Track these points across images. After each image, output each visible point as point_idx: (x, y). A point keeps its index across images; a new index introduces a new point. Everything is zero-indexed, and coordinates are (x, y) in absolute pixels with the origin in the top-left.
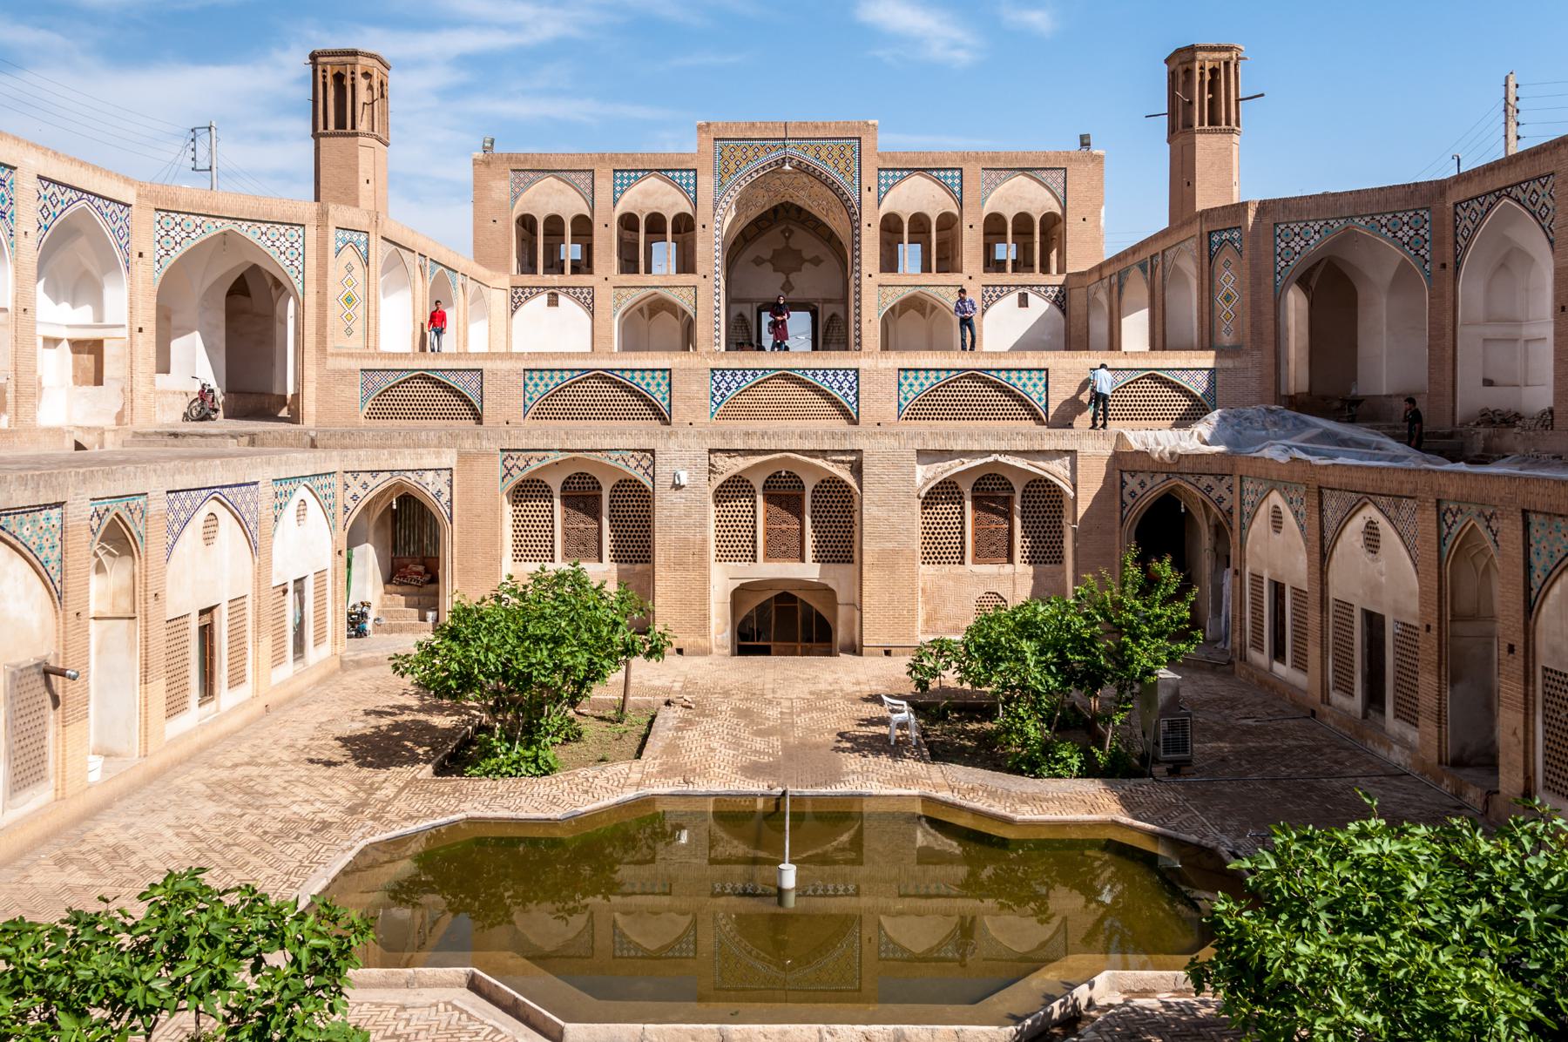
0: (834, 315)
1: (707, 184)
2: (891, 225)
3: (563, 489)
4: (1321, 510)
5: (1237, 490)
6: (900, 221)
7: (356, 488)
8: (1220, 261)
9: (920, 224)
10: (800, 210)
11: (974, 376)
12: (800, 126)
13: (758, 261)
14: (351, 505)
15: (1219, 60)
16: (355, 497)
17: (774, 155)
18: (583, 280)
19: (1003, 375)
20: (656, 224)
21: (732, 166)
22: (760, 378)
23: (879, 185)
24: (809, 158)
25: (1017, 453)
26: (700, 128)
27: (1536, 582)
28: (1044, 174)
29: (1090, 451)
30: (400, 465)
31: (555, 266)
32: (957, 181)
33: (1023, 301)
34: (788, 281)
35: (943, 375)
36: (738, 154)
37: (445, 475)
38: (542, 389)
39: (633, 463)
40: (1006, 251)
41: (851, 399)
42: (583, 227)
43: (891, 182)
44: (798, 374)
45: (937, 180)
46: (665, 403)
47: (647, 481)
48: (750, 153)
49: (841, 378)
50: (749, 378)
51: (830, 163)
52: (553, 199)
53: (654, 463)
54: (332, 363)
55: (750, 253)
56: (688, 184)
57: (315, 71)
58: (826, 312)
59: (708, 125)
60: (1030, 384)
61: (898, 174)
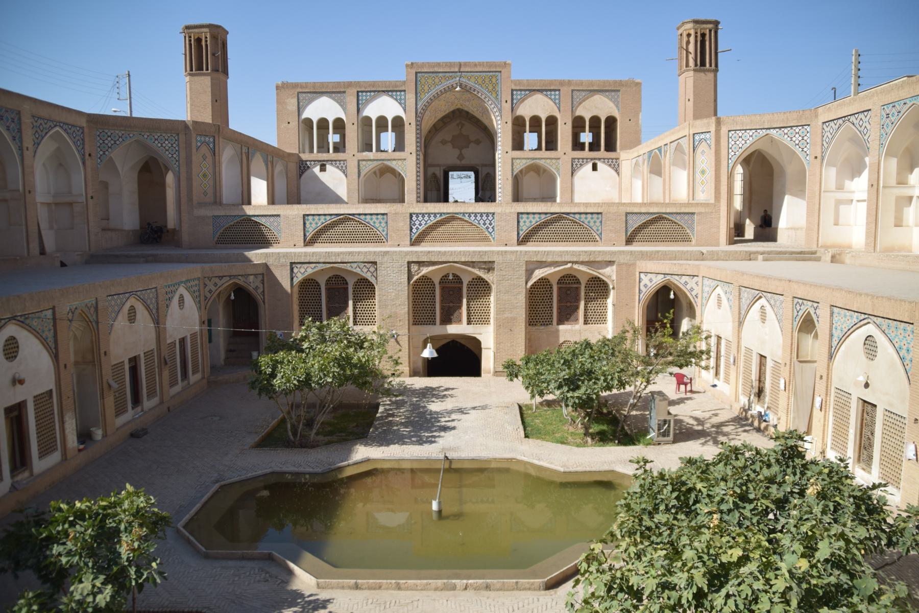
1: (410, 98)
2: (518, 125)
3: (327, 284)
4: (740, 299)
5: (700, 284)
6: (524, 120)
7: (211, 286)
8: (699, 151)
9: (535, 122)
10: (467, 113)
11: (559, 217)
13: (444, 142)
14: (209, 295)
16: (210, 291)
18: (340, 156)
19: (577, 216)
20: (382, 123)
21: (426, 88)
22: (439, 218)
24: (471, 83)
25: (582, 263)
26: (407, 66)
27: (834, 343)
30: (234, 272)
33: (595, 168)
34: (461, 154)
35: (543, 216)
37: (260, 278)
40: (586, 137)
41: (490, 230)
44: (460, 216)
46: (384, 233)
47: (372, 280)
48: (437, 80)
50: (432, 218)
52: (323, 109)
55: (439, 137)
56: (401, 99)
58: (483, 172)
59: (412, 64)
60: (592, 221)
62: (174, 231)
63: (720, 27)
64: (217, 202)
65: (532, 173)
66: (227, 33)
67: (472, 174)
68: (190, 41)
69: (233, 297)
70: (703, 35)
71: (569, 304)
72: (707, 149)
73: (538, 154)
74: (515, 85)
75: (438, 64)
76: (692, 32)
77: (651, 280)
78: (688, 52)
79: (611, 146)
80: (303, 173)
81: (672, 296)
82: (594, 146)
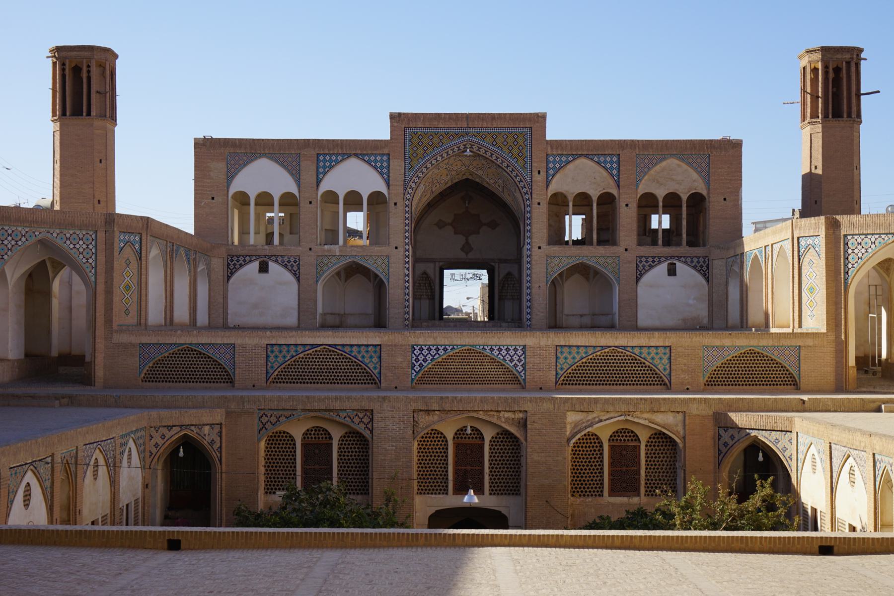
0: (509, 274)
1: (397, 166)
7: (158, 439)
9: (582, 203)
13: (441, 225)
14: (154, 450)
20: (353, 201)
21: (420, 151)
23: (548, 169)
29: (695, 412)
30: (187, 421)
32: (615, 165)
33: (672, 271)
34: (467, 243)
35: (591, 351)
36: (426, 141)
37: (217, 429)
38: (280, 359)
39: (357, 420)
40: (661, 221)
41: (520, 368)
43: (558, 166)
46: (376, 372)
47: (367, 434)
48: (436, 140)
49: (512, 352)
50: (441, 352)
51: (505, 149)
52: (263, 178)
53: (372, 420)
54: (118, 338)
62: (90, 363)
63: (863, 55)
64: (141, 324)
65: (577, 276)
66: (116, 56)
68: (63, 70)
69: (181, 453)
70: (837, 70)
71: (624, 469)
72: (815, 259)
73: (585, 250)
74: (552, 148)
76: (819, 66)
77: (732, 437)
78: (815, 98)
80: (232, 274)
81: (761, 458)
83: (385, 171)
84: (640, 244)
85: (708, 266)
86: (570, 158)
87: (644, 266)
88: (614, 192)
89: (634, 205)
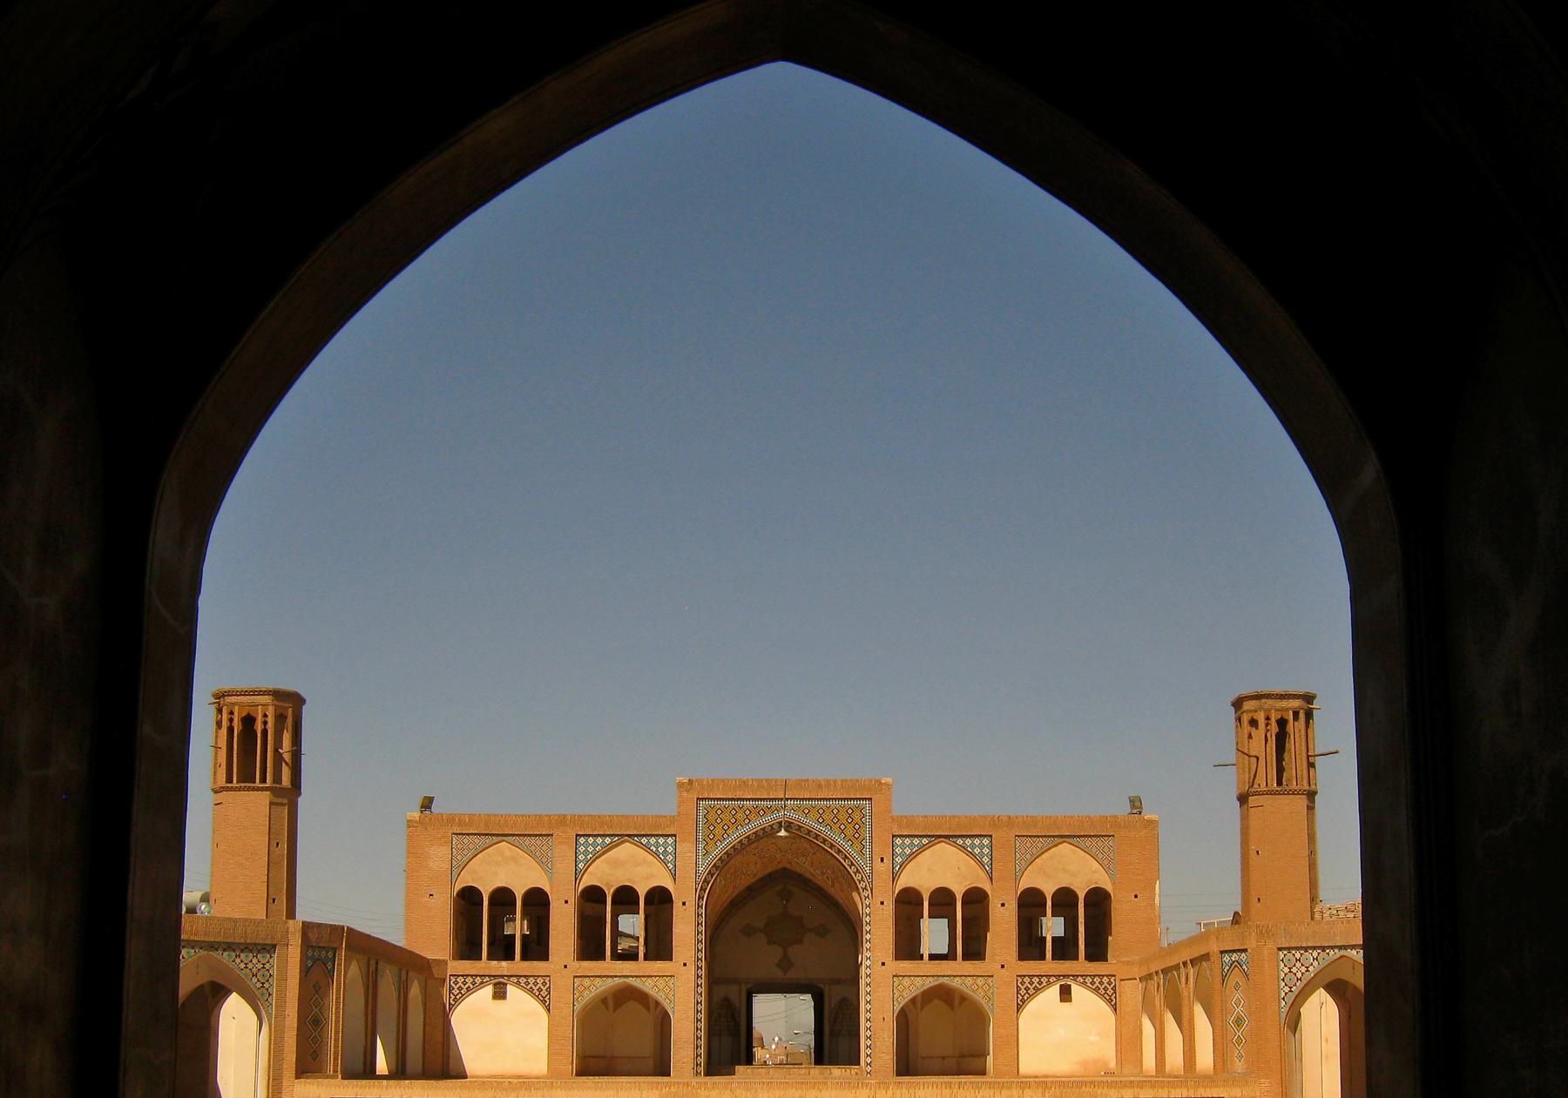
1: (686, 850)
2: (908, 903)
9: (942, 901)
12: (800, 784)
13: (748, 931)
15: (1287, 710)
17: (768, 820)
20: (626, 898)
24: (810, 822)
26: (680, 785)
28: (1088, 842)
31: (503, 949)
32: (986, 851)
33: (1065, 994)
42: (537, 902)
43: (908, 851)
45: (963, 848)
52: (506, 870)
57: (220, 711)
58: (833, 997)
59: (691, 782)
61: (916, 842)
65: (937, 1002)
67: (808, 997)
68: (231, 720)
70: (1282, 723)
74: (900, 826)
75: (744, 784)
79: (1097, 951)
82: (1064, 949)
83: (670, 858)
84: (1022, 957)
85: (1114, 989)
86: (925, 841)
87: (1027, 989)
88: (987, 887)
89: (1012, 906)
